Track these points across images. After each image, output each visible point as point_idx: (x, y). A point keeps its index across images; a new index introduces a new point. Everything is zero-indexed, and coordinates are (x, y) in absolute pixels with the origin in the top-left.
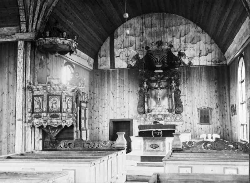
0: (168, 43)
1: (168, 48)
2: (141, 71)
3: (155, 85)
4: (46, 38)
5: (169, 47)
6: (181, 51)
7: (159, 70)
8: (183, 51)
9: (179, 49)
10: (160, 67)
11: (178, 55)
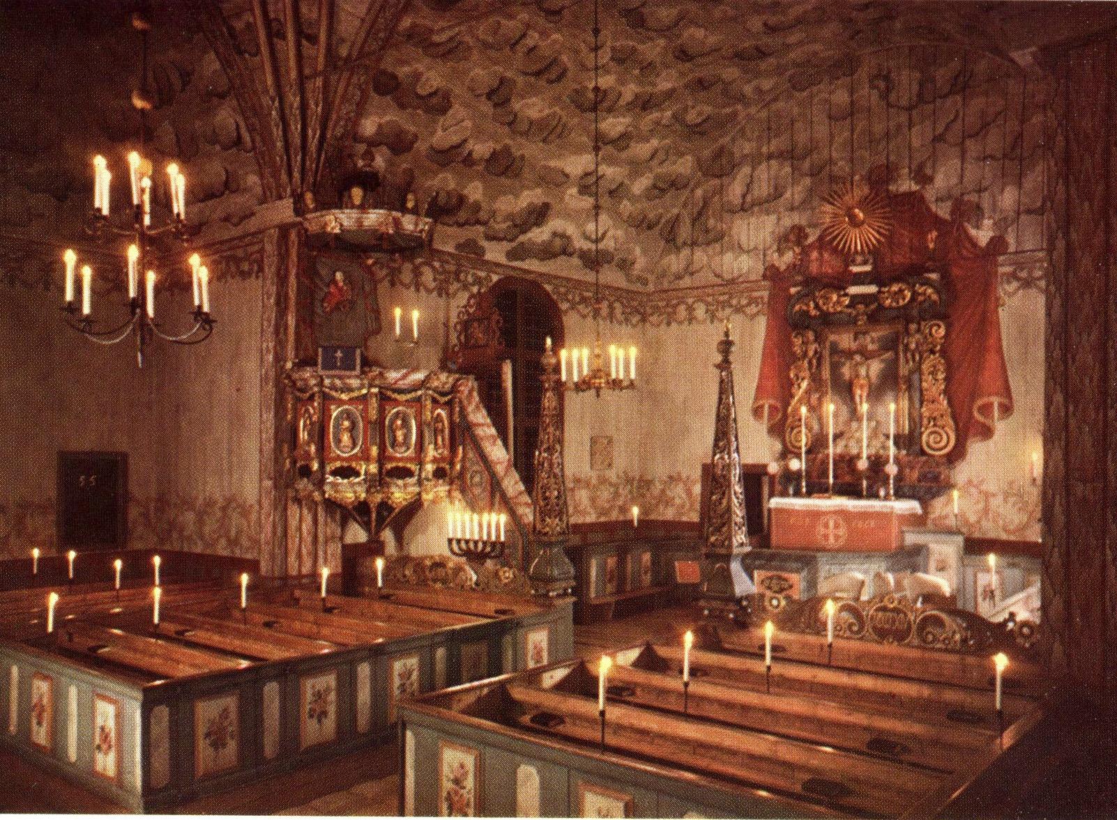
0: (913, 167)
1: (915, 187)
2: (798, 292)
3: (845, 340)
4: (309, 216)
5: (916, 183)
6: (966, 198)
7: (863, 283)
8: (974, 198)
9: (956, 192)
10: (866, 273)
11: (952, 213)
